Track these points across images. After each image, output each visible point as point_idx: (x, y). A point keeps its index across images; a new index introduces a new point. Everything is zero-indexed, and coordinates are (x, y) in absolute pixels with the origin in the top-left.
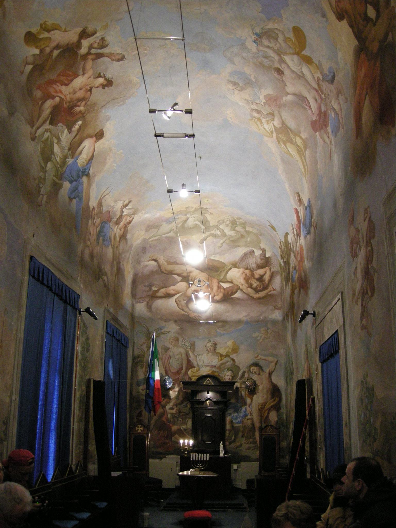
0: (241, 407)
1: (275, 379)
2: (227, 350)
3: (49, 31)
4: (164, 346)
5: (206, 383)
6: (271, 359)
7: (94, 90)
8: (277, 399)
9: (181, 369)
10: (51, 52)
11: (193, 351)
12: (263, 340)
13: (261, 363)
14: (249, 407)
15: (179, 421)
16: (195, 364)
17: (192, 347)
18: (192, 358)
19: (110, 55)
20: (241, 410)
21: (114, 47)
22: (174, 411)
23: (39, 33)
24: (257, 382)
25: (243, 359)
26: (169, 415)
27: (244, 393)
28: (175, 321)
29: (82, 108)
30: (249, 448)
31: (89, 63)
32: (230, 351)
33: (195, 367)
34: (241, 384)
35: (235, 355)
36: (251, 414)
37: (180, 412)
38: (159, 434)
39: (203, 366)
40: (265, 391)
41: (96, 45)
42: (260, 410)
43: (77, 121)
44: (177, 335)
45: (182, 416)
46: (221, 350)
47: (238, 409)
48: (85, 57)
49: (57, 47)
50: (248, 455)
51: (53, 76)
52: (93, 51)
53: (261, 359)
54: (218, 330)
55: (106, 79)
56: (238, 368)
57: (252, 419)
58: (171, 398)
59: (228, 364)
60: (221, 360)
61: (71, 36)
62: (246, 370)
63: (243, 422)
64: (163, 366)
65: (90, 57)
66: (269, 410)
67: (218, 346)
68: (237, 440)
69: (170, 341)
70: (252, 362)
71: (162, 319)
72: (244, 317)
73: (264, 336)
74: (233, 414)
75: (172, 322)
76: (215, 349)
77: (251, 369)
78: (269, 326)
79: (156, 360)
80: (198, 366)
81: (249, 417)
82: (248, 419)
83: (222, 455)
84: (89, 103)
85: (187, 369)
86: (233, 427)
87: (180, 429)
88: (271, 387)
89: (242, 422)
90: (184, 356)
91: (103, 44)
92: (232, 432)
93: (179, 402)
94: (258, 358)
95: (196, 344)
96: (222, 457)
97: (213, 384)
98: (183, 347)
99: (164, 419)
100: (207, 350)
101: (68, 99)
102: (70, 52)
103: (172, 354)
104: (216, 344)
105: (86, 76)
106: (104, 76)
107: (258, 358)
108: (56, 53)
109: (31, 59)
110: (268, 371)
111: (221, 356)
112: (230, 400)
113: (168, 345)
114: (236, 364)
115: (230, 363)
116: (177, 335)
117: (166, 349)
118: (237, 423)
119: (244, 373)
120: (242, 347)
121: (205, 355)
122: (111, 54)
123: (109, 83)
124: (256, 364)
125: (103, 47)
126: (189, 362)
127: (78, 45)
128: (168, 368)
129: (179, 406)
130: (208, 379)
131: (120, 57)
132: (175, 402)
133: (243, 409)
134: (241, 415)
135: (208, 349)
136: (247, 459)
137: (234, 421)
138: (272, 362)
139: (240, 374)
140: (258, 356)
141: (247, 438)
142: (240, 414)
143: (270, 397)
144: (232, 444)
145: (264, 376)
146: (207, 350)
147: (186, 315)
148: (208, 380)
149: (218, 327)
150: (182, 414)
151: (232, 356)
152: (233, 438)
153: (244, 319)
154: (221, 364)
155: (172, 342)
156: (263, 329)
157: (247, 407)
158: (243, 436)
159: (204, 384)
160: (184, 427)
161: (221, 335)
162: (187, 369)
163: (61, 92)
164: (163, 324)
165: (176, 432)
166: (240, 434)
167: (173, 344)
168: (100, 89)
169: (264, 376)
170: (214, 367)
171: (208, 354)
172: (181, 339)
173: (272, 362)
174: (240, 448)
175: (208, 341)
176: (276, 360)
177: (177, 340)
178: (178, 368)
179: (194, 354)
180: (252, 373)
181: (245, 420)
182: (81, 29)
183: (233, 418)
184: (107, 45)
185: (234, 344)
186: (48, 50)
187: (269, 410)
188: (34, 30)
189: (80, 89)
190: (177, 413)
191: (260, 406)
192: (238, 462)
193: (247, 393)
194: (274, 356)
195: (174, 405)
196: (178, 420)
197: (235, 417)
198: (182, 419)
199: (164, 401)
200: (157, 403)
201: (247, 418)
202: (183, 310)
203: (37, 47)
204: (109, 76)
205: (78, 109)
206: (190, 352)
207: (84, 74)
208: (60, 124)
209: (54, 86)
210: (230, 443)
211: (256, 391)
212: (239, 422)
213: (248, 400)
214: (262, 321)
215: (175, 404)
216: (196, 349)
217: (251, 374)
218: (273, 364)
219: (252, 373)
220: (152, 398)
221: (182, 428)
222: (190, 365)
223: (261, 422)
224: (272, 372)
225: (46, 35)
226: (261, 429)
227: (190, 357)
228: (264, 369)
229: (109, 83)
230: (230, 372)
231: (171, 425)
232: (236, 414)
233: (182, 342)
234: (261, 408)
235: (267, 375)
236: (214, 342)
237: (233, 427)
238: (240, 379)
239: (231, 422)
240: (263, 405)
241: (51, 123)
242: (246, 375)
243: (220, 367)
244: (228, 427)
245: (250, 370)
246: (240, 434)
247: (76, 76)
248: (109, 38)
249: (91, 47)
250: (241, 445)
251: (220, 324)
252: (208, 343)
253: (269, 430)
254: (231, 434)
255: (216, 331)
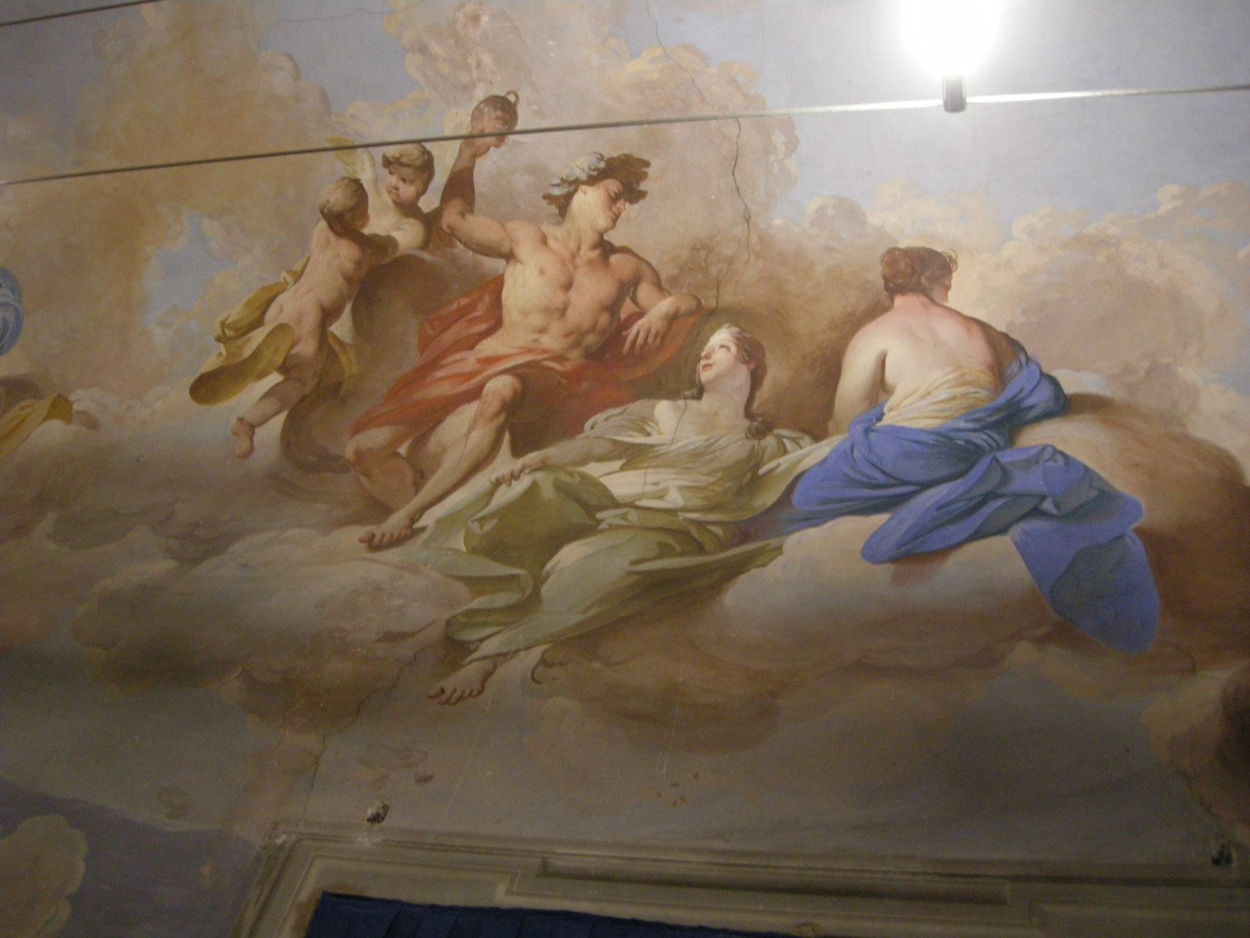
7: (616, 238)
55: (593, 180)
61: (329, 262)
65: (451, 217)
105: (526, 250)
106: (577, 183)
108: (342, 328)
125: (426, 167)
168: (630, 210)
182: (323, 224)
186: (307, 348)
249: (408, 209)
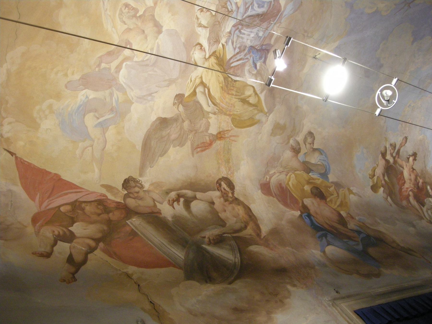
3: (374, 175)
7: (414, 167)
10: (385, 180)
19: (401, 146)
21: (398, 140)
23: (373, 182)
29: (421, 181)
31: (399, 161)
41: (392, 151)
43: (427, 188)
48: (395, 162)
49: (384, 175)
51: (397, 187)
52: (394, 155)
55: (412, 156)
61: (382, 163)
65: (396, 158)
84: (420, 175)
91: (393, 146)
101: (412, 186)
102: (391, 170)
105: (405, 167)
106: (410, 155)
108: (386, 178)
109: (385, 195)
122: (401, 144)
123: (415, 155)
125: (395, 147)
127: (387, 161)
131: (405, 140)
163: (407, 188)
168: (415, 162)
182: (381, 155)
184: (395, 144)
186: (383, 182)
188: (371, 184)
189: (410, 175)
203: (380, 188)
204: (411, 153)
205: (420, 184)
207: (403, 168)
208: (425, 200)
209: (403, 190)
225: (375, 178)
229: (415, 155)
241: (424, 206)
247: (402, 173)
248: (392, 142)
249: (392, 155)
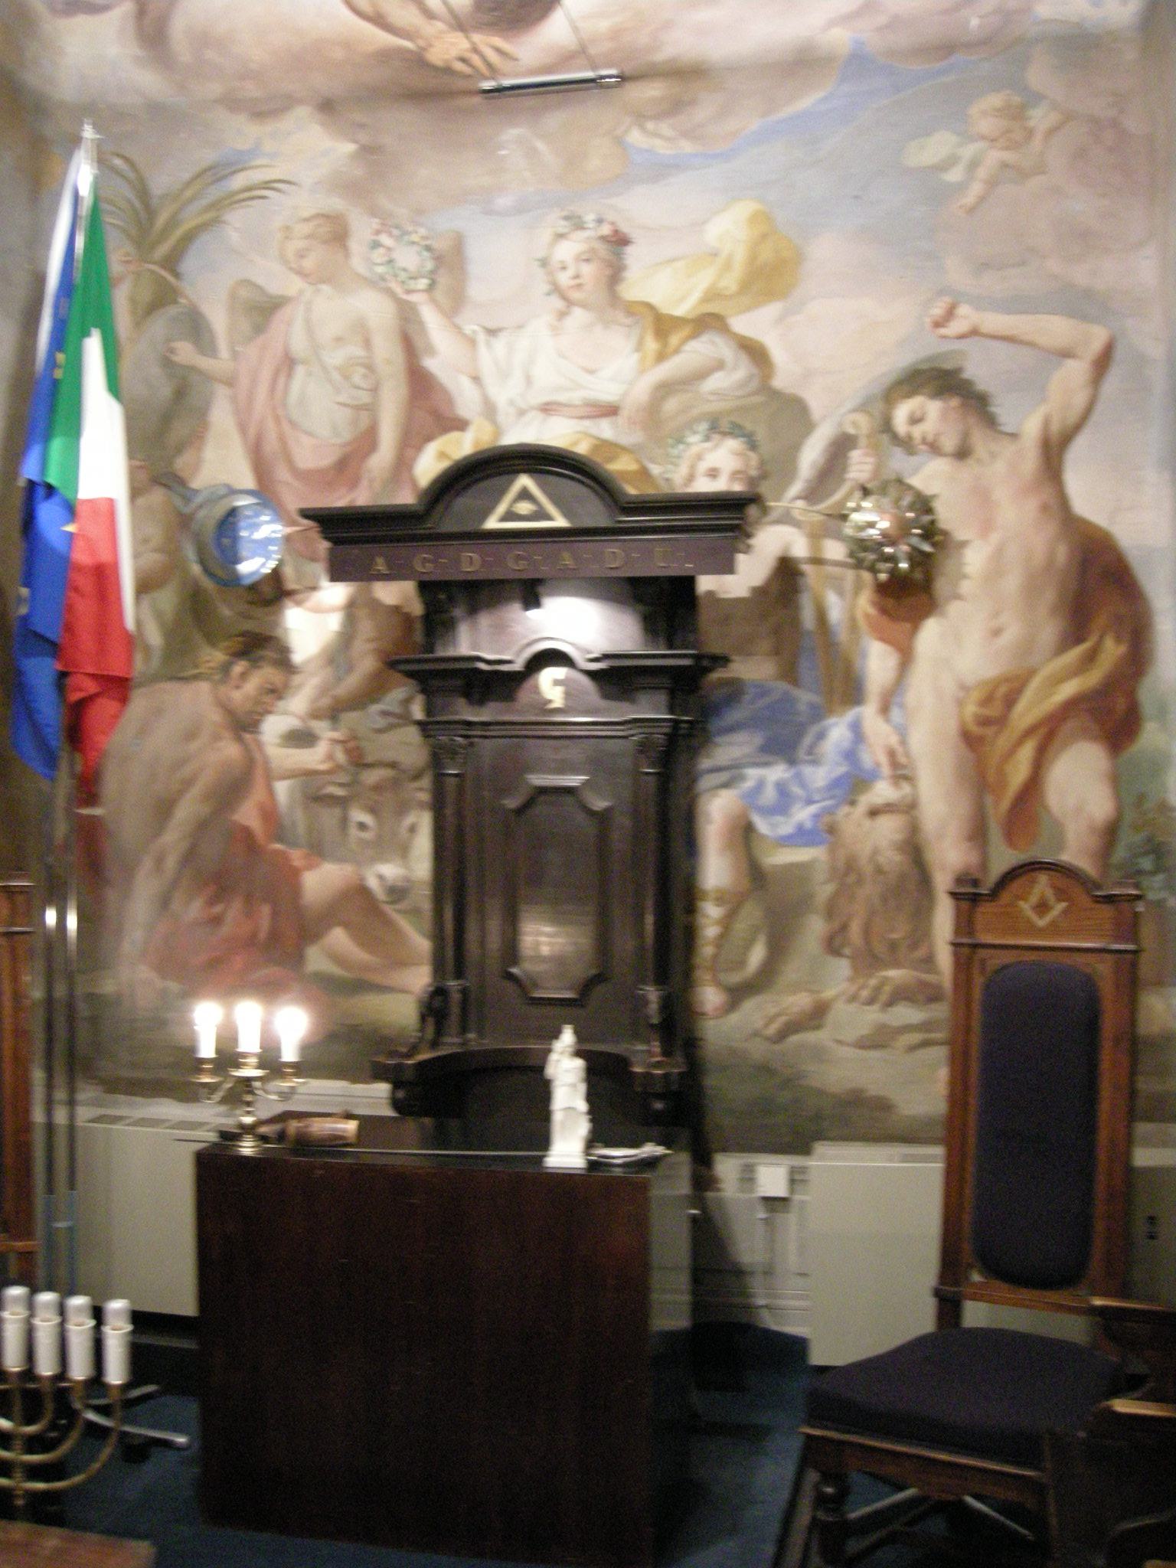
0: (818, 714)
1: (1089, 493)
2: (704, 280)
4: (244, 293)
5: (510, 516)
6: (1055, 329)
8: (1113, 651)
9: (367, 441)
11: (455, 303)
12: (992, 183)
13: (978, 370)
14: (885, 709)
15: (353, 832)
16: (466, 399)
17: (443, 280)
18: (444, 360)
20: (821, 736)
22: (314, 757)
24: (947, 515)
25: (837, 342)
26: (283, 790)
27: (842, 602)
28: (327, 107)
30: (878, 1040)
32: (730, 283)
33: (461, 425)
34: (816, 536)
35: (772, 310)
36: (902, 773)
37: (358, 761)
38: (216, 921)
39: (522, 413)
40: (1012, 583)
42: (972, 740)
44: (335, 203)
45: (378, 788)
46: (662, 282)
47: (800, 731)
50: (873, 1090)
53: (974, 332)
54: (635, 137)
56: (794, 414)
57: (909, 808)
58: (298, 657)
59: (716, 382)
60: (661, 357)
62: (862, 425)
63: (832, 830)
64: (243, 428)
66: (1049, 735)
67: (634, 256)
68: (792, 970)
69: (292, 247)
70: (904, 360)
71: (233, 103)
72: (832, 23)
73: (994, 156)
74: (753, 774)
75: (302, 112)
76: (615, 274)
77: (901, 414)
78: (1039, 75)
79: (93, 348)
80: (490, 410)
81: (883, 791)
82: (874, 813)
83: (567, 1150)
85: (411, 441)
86: (756, 876)
87: (362, 891)
88: (1062, 553)
89: (827, 831)
90: (387, 352)
92: (752, 913)
93: (353, 681)
94: (956, 327)
95: (476, 252)
96: (565, 1180)
97: (560, 522)
98: (376, 283)
99: (247, 814)
100: (556, 289)
103: (299, 344)
104: (619, 241)
107: (956, 327)
110: (1031, 428)
111: (663, 325)
112: (722, 660)
113: (277, 280)
114: (779, 382)
115: (729, 379)
116: (335, 203)
117: (263, 310)
118: (787, 841)
119: (841, 446)
120: (827, 251)
121: (540, 326)
124: (941, 380)
126: (421, 385)
128: (271, 445)
129: (350, 718)
130: (525, 481)
132: (324, 690)
133: (837, 731)
134: (819, 776)
135: (564, 279)
136: (861, 1119)
137: (762, 825)
138: (1066, 354)
139: (811, 455)
140: (950, 314)
141: (868, 960)
142: (808, 770)
143: (1049, 632)
144: (749, 1005)
145: (1000, 467)
146: (556, 289)
147: (400, 51)
148: (524, 495)
149: (640, 117)
150: (372, 777)
151: (742, 324)
152: (757, 955)
153: (840, 38)
154: (665, 389)
155: (301, 255)
156: (995, 100)
157: (868, 712)
158: (833, 946)
159: (492, 523)
160: (390, 870)
161: (660, 170)
162: (411, 441)
164: (240, 133)
165: (333, 913)
166: (815, 927)
167: (308, 264)
169: (1005, 468)
170: (610, 411)
171: (562, 315)
172: (362, 228)
173: (1066, 354)
174: (810, 1037)
175: (563, 226)
176: (1097, 337)
177: (337, 234)
178: (347, 435)
179: (458, 329)
180: (906, 444)
181: (852, 820)
183: (740, 799)
185: (764, 226)
187: (1049, 735)
190: (339, 768)
191: (971, 709)
192: (795, 1139)
193: (865, 603)
194: (1080, 304)
195: (315, 715)
196: (344, 821)
197: (769, 795)
198: (373, 810)
199: (252, 685)
200: (91, 687)
201: (867, 800)
202: (378, 20)
206: (430, 317)
210: (737, 995)
211: (941, 586)
212: (802, 836)
213: (877, 662)
214: (985, 43)
215: (326, 702)
216: (476, 290)
217: (898, 452)
218: (1077, 371)
219: (906, 444)
220: (54, 649)
221: (373, 883)
222: (428, 406)
223: (978, 833)
224: (1067, 438)
226: (970, 896)
227: (431, 351)
228: (1004, 410)
230: (733, 444)
231: (297, 857)
232: (777, 773)
233: (376, 245)
234: (985, 722)
235: (1030, 461)
236: (606, 230)
237: (756, 876)
238: (814, 493)
239: (744, 834)
240: (1002, 695)
242: (860, 466)
243: (652, 414)
244: (716, 869)
245: (886, 426)
246: (815, 927)
250: (817, 1015)
251: (651, 91)
252: (561, 236)
253: (1042, 907)
254: (741, 926)
255: (619, 141)
